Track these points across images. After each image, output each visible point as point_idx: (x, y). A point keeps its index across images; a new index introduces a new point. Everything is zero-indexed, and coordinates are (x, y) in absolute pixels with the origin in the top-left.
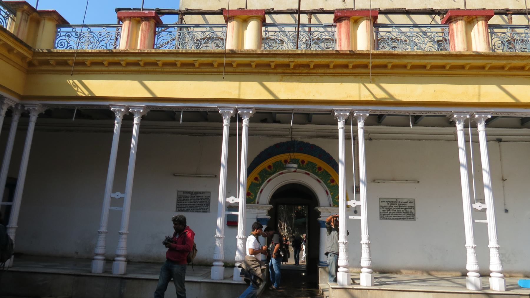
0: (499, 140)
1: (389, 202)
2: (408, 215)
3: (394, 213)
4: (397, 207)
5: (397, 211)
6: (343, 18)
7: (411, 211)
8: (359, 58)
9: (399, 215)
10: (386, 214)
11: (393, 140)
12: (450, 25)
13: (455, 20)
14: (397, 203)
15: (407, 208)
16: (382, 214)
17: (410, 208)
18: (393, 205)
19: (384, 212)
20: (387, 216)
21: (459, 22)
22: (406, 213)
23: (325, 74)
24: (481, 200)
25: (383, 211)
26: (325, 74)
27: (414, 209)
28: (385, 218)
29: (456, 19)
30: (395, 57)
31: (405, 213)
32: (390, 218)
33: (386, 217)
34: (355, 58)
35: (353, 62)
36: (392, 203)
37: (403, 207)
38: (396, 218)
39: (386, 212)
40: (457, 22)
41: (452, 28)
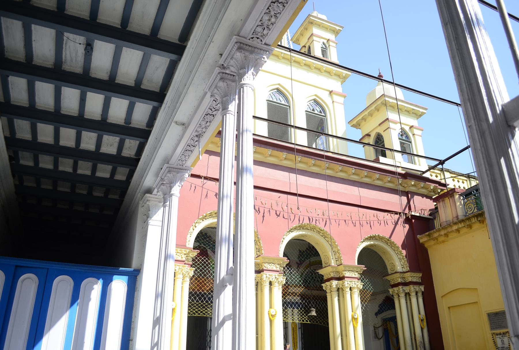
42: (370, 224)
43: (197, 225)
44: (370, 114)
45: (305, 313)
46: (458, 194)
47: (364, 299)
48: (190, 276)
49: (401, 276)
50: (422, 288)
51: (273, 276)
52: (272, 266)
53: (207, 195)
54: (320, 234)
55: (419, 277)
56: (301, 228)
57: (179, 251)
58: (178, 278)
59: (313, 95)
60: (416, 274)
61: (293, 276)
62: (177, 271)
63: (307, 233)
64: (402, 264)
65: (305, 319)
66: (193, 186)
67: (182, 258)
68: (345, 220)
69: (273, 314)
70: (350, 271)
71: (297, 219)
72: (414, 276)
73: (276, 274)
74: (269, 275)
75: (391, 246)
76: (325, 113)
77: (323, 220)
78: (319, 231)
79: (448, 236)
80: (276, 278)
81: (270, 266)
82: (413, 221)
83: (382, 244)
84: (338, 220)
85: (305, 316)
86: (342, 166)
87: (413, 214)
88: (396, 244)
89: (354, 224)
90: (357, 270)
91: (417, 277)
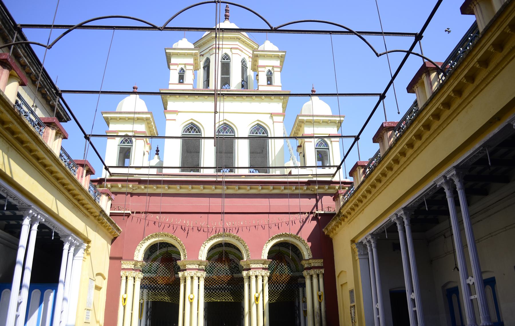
6: (8, 66)
8: (19, 124)
13: (53, 127)
29: (54, 127)
30: (36, 140)
34: (17, 122)
41: (48, 132)
42: (278, 226)
44: (298, 129)
45: (230, 294)
46: (342, 195)
47: (270, 282)
48: (139, 278)
49: (307, 262)
51: (193, 273)
52: (193, 266)
56: (220, 236)
57: (128, 263)
58: (129, 280)
59: (256, 121)
61: (222, 269)
62: (127, 275)
63: (225, 239)
64: (308, 252)
65: (230, 299)
66: (139, 219)
67: (131, 267)
69: (191, 298)
70: (256, 263)
71: (214, 231)
72: (316, 262)
73: (195, 271)
74: (190, 272)
76: (267, 133)
77: (236, 229)
78: (234, 237)
79: (335, 230)
80: (195, 274)
81: (191, 266)
85: (230, 297)
86: (249, 186)
87: (317, 212)
89: (263, 228)
90: (262, 263)
91: (319, 262)
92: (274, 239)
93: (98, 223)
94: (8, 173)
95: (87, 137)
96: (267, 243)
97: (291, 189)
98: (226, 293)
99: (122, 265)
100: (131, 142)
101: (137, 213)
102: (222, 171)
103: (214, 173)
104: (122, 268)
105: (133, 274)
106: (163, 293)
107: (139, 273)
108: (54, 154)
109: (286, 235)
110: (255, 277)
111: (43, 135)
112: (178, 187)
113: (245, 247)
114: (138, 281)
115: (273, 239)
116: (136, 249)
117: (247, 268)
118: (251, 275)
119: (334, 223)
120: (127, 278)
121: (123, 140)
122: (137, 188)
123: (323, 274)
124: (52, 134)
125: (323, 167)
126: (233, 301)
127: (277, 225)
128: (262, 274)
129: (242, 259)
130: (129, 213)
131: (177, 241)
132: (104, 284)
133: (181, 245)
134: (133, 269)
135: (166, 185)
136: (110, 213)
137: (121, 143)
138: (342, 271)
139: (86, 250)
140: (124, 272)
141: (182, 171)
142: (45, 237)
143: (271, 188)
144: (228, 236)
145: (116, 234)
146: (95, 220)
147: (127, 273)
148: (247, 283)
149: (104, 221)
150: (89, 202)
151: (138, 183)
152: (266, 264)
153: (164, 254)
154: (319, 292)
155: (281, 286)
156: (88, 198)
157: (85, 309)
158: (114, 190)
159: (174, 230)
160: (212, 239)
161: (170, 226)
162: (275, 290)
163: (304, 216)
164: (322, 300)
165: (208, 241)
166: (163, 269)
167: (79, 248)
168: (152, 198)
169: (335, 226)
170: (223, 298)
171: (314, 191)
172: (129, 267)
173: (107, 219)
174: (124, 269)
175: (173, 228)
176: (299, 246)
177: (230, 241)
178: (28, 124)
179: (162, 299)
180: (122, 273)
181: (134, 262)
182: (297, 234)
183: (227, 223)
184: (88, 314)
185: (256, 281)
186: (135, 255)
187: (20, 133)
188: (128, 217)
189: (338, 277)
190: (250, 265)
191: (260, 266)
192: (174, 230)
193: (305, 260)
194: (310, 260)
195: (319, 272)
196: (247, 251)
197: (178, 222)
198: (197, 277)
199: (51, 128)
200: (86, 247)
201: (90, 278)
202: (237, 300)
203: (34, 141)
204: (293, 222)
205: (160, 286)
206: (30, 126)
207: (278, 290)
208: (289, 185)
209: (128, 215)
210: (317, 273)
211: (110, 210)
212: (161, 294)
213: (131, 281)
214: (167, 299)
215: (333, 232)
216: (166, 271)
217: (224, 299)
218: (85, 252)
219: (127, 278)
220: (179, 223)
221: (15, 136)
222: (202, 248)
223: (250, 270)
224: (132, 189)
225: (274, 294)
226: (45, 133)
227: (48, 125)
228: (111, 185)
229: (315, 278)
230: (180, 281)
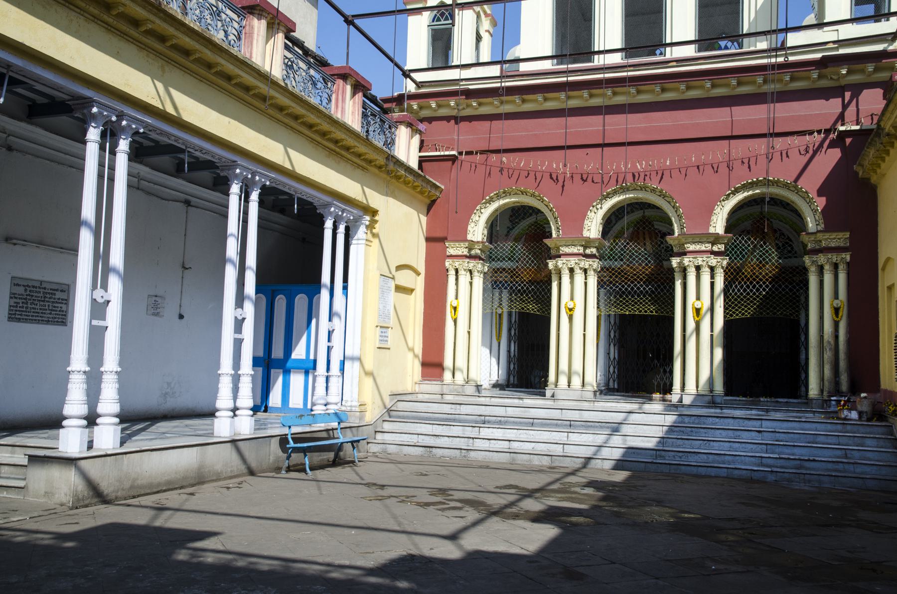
0: (188, 203)
1: (28, 286)
2: (55, 314)
3: (34, 308)
4: (40, 299)
5: (38, 305)
7: (61, 307)
8: (165, 21)
9: (42, 313)
10: (19, 311)
11: (48, 162)
12: (248, 16)
13: (259, 14)
14: (42, 290)
15: (55, 301)
16: (12, 310)
17: (60, 301)
18: (35, 294)
19: (17, 306)
20: (21, 315)
21: (262, 21)
22: (54, 310)
23: (96, 20)
24: (156, 296)
25: (15, 305)
26: (95, 19)
27: (66, 304)
28: (16, 319)
29: (261, 13)
30: (211, 46)
31: (51, 310)
32: (26, 319)
33: (19, 317)
34: (160, 18)
35: (154, 23)
36: (33, 289)
37: (50, 298)
38: (36, 320)
39: (20, 307)
40: (261, 19)
42: (749, 163)
43: (482, 210)
45: (649, 301)
49: (813, 239)
50: (847, 257)
51: (572, 261)
53: (490, 173)
54: (657, 193)
55: (846, 238)
56: (625, 190)
60: (836, 234)
65: (649, 309)
66: (473, 165)
68: (698, 167)
69: (570, 307)
70: (696, 242)
71: (613, 180)
72: (831, 237)
73: (576, 259)
74: (567, 260)
75: (796, 191)
77: (657, 173)
78: (653, 191)
79: (879, 166)
80: (576, 263)
82: (848, 141)
83: (779, 190)
84: (686, 169)
85: (649, 305)
87: (842, 128)
88: (801, 188)
89: (716, 169)
91: (839, 239)
92: (738, 191)
93: (389, 178)
94: (170, 110)
95: (349, 21)
96: (723, 200)
97: (782, 80)
98: (641, 299)
99: (448, 249)
100: (452, 17)
101: (468, 153)
102: (658, 52)
103: (622, 61)
104: (448, 254)
105: (467, 265)
106: (524, 297)
107: (478, 263)
108: (254, 66)
109: (767, 183)
110: (694, 269)
111: (243, 32)
112: (539, 97)
113: (676, 209)
114: (478, 277)
115: (736, 191)
116: (471, 221)
117: (681, 251)
118: (686, 264)
119: (871, 152)
120: (457, 271)
121: (436, 15)
122: (465, 106)
123: (848, 264)
124: (259, 28)
125: (876, 18)
126: (654, 313)
127: (746, 161)
128: (710, 264)
129: (672, 232)
130: (454, 155)
131: (544, 202)
132: (419, 284)
133: (551, 211)
134: (466, 257)
135: (517, 96)
136: (420, 157)
137: (433, 21)
138: (888, 259)
139: (371, 227)
140: (451, 263)
141: (558, 64)
142: (306, 207)
143: (734, 82)
144: (641, 190)
145: (431, 194)
146: (381, 173)
147: (457, 263)
148: (680, 281)
149: (398, 174)
150: (356, 144)
151: (464, 97)
152: (720, 244)
153: (530, 227)
154: (836, 301)
155: (754, 287)
156: (353, 135)
157: (377, 326)
158: (425, 113)
159: (538, 181)
160: (610, 196)
161: (529, 174)
162: (742, 294)
163: (817, 138)
164: (842, 317)
165: (601, 200)
166: (524, 254)
167: (358, 223)
168: (496, 124)
169: (876, 157)
170: (635, 307)
171: (838, 79)
172: (460, 253)
173: (405, 170)
174: (451, 256)
175: (536, 179)
176: (796, 204)
177: (646, 199)
178: (183, 20)
179: (523, 309)
180: (448, 262)
181: (467, 244)
182: (796, 180)
183: (638, 164)
184: (383, 334)
185: (696, 276)
186: (468, 232)
187: (174, 36)
188: (453, 163)
189: (883, 269)
190: (686, 246)
191: (705, 247)
192: (538, 181)
193: (808, 234)
194: (818, 235)
195: (839, 259)
196: (679, 216)
197: (542, 168)
198: (581, 269)
199: (257, 15)
200: (369, 221)
201: (381, 275)
202: (662, 313)
203: (207, 48)
204: (785, 154)
205: (520, 285)
206: (187, 23)
207: (748, 294)
208: (777, 73)
209: (453, 159)
210: (834, 260)
211: (420, 152)
212: (521, 300)
213: (464, 278)
214: (532, 308)
215: (875, 172)
216: (530, 259)
217: (638, 309)
218: (369, 232)
219: (457, 271)
220: (544, 168)
221: (168, 44)
222: (590, 215)
223: (686, 255)
224: (455, 109)
225: (739, 302)
226: (247, 27)
227: (250, 11)
228: (418, 105)
229: (828, 272)
230: (551, 277)
